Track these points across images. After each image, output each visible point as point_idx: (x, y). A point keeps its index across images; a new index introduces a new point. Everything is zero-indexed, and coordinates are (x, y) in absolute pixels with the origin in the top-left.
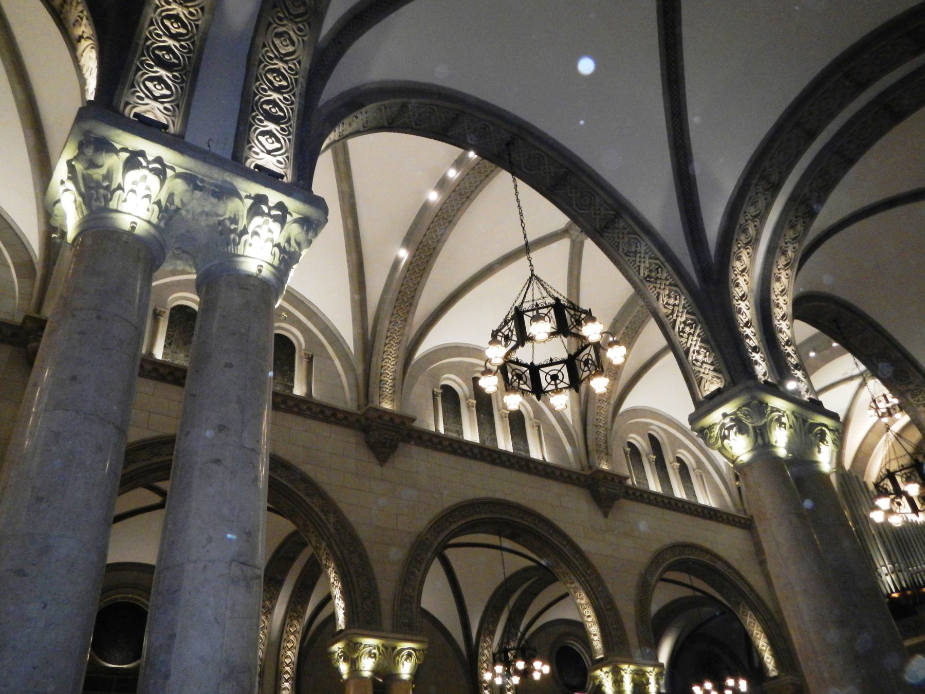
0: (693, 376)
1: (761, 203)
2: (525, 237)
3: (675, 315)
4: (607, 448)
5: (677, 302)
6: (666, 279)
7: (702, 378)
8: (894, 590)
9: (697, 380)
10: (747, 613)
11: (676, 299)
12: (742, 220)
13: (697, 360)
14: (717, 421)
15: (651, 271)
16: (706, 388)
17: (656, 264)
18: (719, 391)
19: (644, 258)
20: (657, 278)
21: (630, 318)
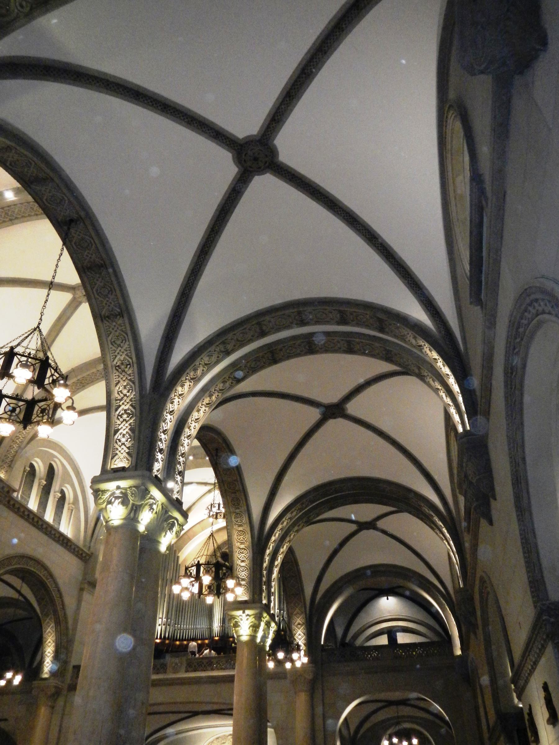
0: (112, 449)
1: (214, 359)
2: (48, 294)
3: (122, 402)
4: (12, 461)
5: (128, 394)
6: (130, 375)
7: (117, 454)
8: (159, 637)
9: (112, 454)
10: (51, 624)
11: (128, 392)
12: (197, 363)
13: (120, 441)
14: (111, 489)
15: (122, 364)
16: (115, 463)
17: (128, 361)
18: (123, 469)
19: (123, 352)
20: (124, 371)
21: (85, 375)
